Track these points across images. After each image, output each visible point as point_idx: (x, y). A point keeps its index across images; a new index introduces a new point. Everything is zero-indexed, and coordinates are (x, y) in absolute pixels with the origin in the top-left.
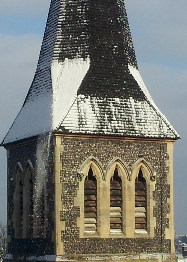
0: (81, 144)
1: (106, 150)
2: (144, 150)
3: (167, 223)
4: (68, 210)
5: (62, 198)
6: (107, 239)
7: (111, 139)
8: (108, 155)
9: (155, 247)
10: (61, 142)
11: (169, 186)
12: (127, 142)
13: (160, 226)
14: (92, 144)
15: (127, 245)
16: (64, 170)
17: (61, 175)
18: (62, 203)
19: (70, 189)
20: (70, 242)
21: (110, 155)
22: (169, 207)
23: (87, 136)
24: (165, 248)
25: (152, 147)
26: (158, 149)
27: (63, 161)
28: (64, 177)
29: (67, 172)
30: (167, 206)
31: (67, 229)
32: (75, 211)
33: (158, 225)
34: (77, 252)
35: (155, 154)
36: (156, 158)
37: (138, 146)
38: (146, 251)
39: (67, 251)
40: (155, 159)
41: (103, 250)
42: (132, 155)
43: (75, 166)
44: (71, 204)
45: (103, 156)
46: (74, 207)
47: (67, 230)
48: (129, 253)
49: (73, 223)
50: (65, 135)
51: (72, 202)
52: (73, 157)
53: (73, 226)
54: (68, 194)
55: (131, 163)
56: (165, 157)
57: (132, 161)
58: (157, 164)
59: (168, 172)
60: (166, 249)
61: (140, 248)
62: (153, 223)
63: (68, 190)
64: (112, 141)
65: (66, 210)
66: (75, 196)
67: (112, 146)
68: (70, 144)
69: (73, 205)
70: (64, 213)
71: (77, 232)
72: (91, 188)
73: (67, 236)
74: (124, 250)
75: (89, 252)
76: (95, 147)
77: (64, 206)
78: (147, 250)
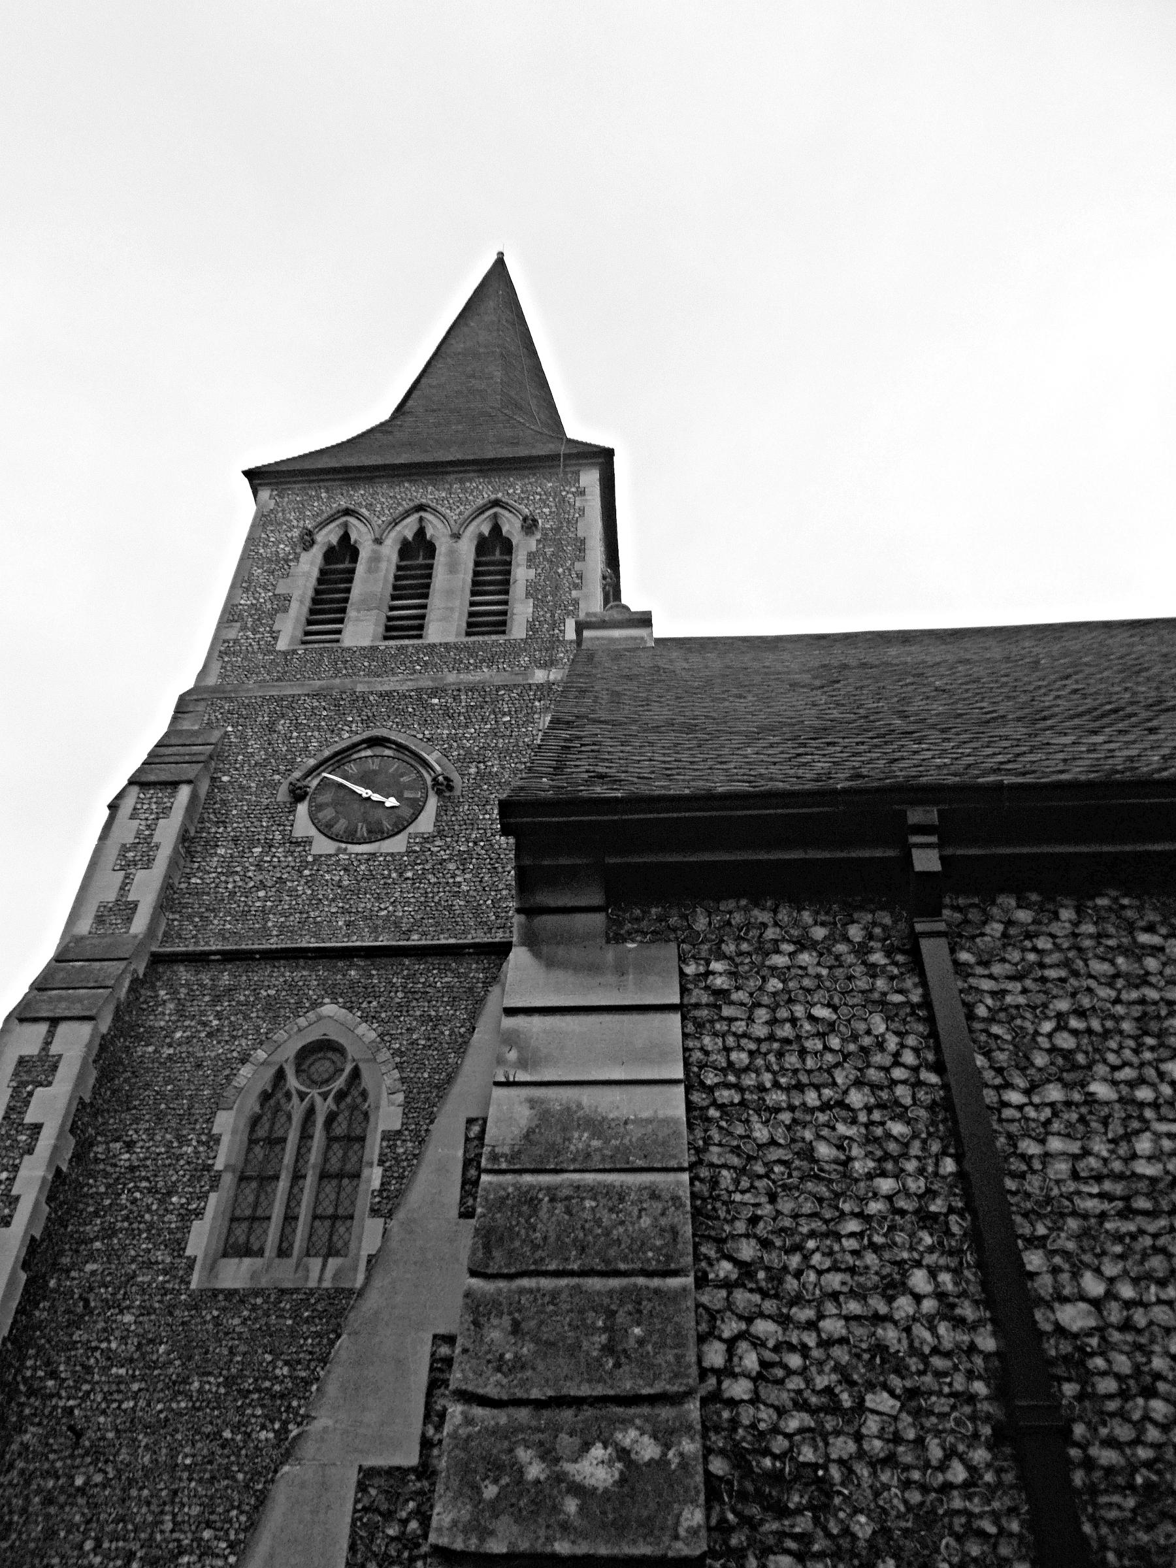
0: (323, 495)
6: (364, 648)
13: (548, 615)
14: (356, 491)
24: (562, 659)
37: (489, 483)
56: (573, 493)
58: (549, 507)
62: (522, 611)
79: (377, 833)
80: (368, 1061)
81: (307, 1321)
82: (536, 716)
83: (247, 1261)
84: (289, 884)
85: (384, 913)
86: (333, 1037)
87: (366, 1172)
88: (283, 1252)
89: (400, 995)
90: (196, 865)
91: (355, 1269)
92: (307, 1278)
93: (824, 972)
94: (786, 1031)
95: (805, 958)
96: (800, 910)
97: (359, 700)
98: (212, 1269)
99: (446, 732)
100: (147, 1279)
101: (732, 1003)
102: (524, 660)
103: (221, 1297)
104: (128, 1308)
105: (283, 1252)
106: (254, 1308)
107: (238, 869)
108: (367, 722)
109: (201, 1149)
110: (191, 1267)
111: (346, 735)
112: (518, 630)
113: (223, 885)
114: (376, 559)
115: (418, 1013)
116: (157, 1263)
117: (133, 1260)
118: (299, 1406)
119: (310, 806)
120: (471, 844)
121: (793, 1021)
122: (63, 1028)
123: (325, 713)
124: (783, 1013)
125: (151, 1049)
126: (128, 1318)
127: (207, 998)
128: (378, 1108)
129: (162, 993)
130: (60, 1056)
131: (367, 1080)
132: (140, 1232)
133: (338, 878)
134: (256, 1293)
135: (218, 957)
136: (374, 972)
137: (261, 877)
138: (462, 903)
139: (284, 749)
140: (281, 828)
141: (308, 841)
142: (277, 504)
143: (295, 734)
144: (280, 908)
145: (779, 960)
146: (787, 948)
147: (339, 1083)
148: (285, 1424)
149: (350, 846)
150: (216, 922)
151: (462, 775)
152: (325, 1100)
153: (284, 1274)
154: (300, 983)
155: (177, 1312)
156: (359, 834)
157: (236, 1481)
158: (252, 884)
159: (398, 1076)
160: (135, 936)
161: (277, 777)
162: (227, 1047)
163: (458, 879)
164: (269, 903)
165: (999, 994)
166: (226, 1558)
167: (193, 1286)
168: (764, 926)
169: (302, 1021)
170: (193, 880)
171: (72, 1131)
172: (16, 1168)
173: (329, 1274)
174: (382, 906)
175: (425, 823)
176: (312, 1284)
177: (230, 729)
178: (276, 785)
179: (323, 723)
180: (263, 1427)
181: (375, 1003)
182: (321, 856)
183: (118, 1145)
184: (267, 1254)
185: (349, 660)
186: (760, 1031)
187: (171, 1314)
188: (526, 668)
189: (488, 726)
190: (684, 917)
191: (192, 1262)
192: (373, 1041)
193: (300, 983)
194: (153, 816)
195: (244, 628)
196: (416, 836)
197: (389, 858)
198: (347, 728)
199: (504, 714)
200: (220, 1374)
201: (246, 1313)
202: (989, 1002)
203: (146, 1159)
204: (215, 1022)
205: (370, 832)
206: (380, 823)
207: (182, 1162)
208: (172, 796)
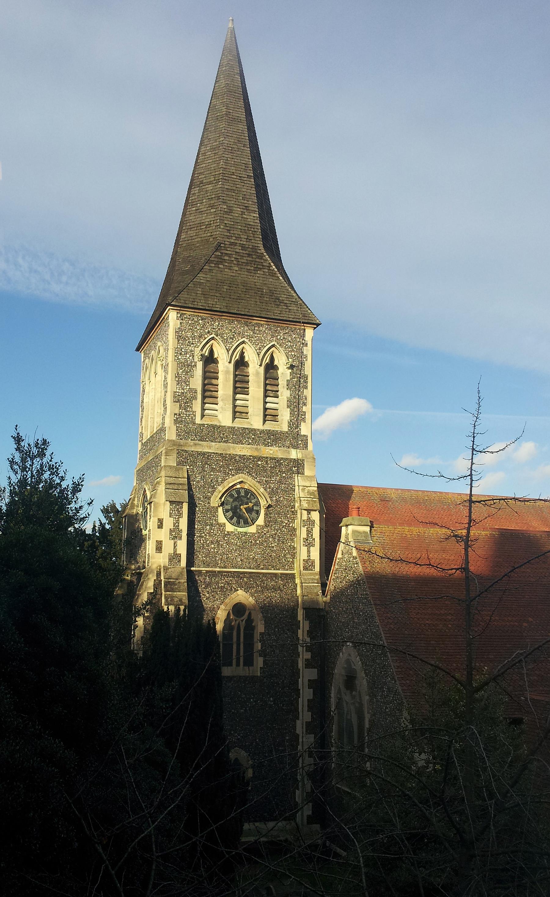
0: (200, 321)
1: (231, 331)
2: (277, 334)
3: (303, 417)
5: (176, 377)
6: (229, 427)
7: (237, 319)
9: (288, 442)
10: (177, 317)
11: (307, 376)
12: (256, 324)
15: (253, 437)
16: (179, 347)
17: (175, 353)
18: (176, 383)
19: (187, 369)
20: (184, 426)
21: (235, 335)
23: (208, 312)
24: (300, 444)
25: (287, 331)
26: (294, 334)
28: (179, 355)
29: (183, 350)
30: (304, 398)
31: (181, 412)
32: (191, 393)
33: (293, 418)
34: (192, 438)
35: (290, 339)
37: (270, 329)
38: (277, 445)
39: (180, 435)
40: (290, 345)
41: (224, 440)
42: (263, 338)
43: (192, 344)
44: (186, 385)
45: (228, 336)
46: (190, 388)
47: (180, 413)
48: (256, 445)
49: (188, 406)
50: (181, 309)
51: (187, 383)
52: (191, 334)
53: (188, 409)
54: (184, 373)
55: (261, 346)
57: (262, 344)
58: (293, 351)
59: (307, 360)
60: (301, 445)
63: (183, 369)
64: (237, 320)
65: (180, 391)
66: (192, 376)
67: (239, 326)
68: (188, 320)
69: (189, 386)
70: (177, 394)
71: (192, 415)
72: (212, 370)
73: (181, 419)
74: (250, 441)
75: (207, 439)
77: (178, 386)
78: (278, 444)
79: (246, 524)
81: (247, 684)
84: (221, 543)
85: (251, 557)
87: (256, 645)
88: (238, 665)
97: (232, 457)
99: (264, 479)
107: (203, 535)
111: (231, 476)
113: (199, 541)
114: (227, 372)
115: (265, 595)
118: (248, 705)
119: (223, 510)
120: (276, 531)
127: (203, 586)
134: (234, 677)
136: (251, 579)
138: (275, 555)
139: (210, 480)
140: (214, 518)
141: (224, 524)
143: (212, 473)
144: (219, 552)
147: (245, 617)
148: (246, 708)
149: (238, 528)
150: (200, 556)
152: (242, 621)
156: (241, 524)
157: (237, 721)
158: (208, 542)
159: (262, 615)
162: (212, 604)
163: (273, 545)
166: (237, 737)
174: (251, 554)
175: (261, 521)
177: (188, 467)
179: (221, 469)
180: (241, 709)
181: (253, 590)
182: (229, 532)
189: (278, 478)
192: (254, 603)
197: (251, 535)
199: (284, 472)
200: (229, 697)
204: (208, 595)
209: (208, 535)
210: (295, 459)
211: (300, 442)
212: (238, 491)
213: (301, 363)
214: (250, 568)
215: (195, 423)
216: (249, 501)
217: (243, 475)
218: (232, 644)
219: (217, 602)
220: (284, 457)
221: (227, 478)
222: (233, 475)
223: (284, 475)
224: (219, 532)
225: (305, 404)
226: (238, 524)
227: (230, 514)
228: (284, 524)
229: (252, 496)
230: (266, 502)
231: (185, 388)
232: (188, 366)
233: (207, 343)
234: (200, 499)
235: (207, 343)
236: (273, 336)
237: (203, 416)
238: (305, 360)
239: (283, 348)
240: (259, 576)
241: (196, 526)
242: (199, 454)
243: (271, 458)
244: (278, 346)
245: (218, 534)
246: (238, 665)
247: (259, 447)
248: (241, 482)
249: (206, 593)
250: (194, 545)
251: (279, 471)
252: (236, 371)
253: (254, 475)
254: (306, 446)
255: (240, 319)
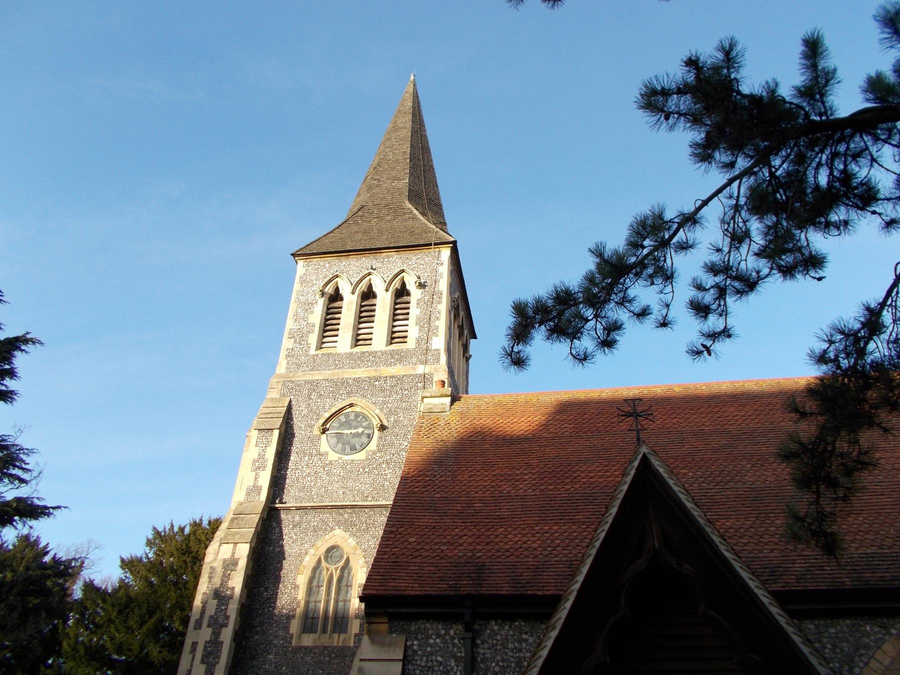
0: (327, 265)
1: (358, 267)
4: (299, 327)
8: (360, 271)
15: (373, 359)
18: (293, 321)
22: (439, 313)
27: (303, 281)
36: (425, 267)
37: (401, 258)
42: (392, 267)
53: (303, 343)
61: (392, 360)
65: (297, 328)
71: (307, 348)
76: (345, 265)
79: (354, 449)
80: (353, 554)
82: (419, 391)
83: (311, 635)
85: (357, 488)
86: (339, 543)
87: (352, 601)
89: (364, 525)
90: (283, 465)
91: (350, 639)
92: (333, 642)
93: (442, 645)
94: (430, 664)
95: (438, 640)
96: (438, 624)
97: (344, 382)
98: (299, 638)
99: (382, 399)
100: (276, 642)
101: (417, 655)
102: (414, 360)
103: (303, 649)
104: (271, 653)
105: (324, 631)
106: (315, 653)
108: (349, 394)
109: (293, 591)
110: (291, 638)
111: (340, 401)
112: (411, 343)
113: (294, 474)
114: (350, 303)
115: (371, 533)
116: (280, 636)
117: (271, 634)
120: (392, 456)
121: (432, 661)
122: (239, 545)
123: (331, 389)
124: (430, 659)
125: (271, 548)
126: (271, 657)
127: (291, 526)
128: (357, 574)
129: (274, 524)
130: (239, 559)
131: (352, 563)
132: (273, 625)
133: (338, 472)
134: (315, 647)
135: (294, 508)
137: (308, 471)
140: (315, 447)
141: (327, 454)
142: (306, 270)
143: (319, 400)
145: (431, 641)
146: (434, 637)
147: (342, 564)
150: (292, 492)
151: (388, 421)
153: (325, 640)
154: (326, 520)
155: (288, 655)
156: (346, 451)
158: (305, 474)
160: (262, 502)
161: (313, 422)
163: (387, 472)
164: (312, 483)
165: (484, 654)
167: (293, 645)
168: (429, 629)
169: (327, 537)
170: (282, 472)
171: (246, 587)
172: (227, 604)
173: (341, 640)
174: (357, 485)
175: (373, 446)
176: (335, 644)
177: (292, 397)
178: (312, 426)
181: (354, 529)
183: (262, 589)
184: (319, 632)
185: (339, 361)
186: (423, 664)
187: (286, 655)
188: (415, 364)
190: (408, 625)
191: (292, 635)
193: (326, 520)
194: (265, 445)
195: (295, 342)
196: (370, 451)
197: (359, 462)
198: (340, 397)
201: (312, 655)
202: (481, 656)
203: (273, 594)
204: (295, 537)
205: (351, 450)
206: (354, 445)
207: (286, 596)
208: (271, 435)
209: (305, 467)
210: (421, 374)
211: (430, 357)
212: (347, 415)
213: (435, 281)
214: (354, 501)
215: (307, 355)
216: (358, 424)
217: (356, 398)
218: (320, 602)
219: (306, 546)
220: (408, 374)
221: (336, 403)
222: (344, 399)
223: (406, 392)
224: (319, 462)
225: (437, 319)
226: (343, 452)
227: (334, 440)
228: (403, 447)
229: (363, 419)
230: (379, 422)
231: (303, 323)
232: (308, 304)
233: (330, 281)
234: (300, 428)
235: (330, 281)
236: (403, 263)
237: (319, 347)
238: (439, 277)
239: (415, 272)
240: (365, 511)
241: (292, 458)
242: (307, 382)
243: (390, 377)
244: (407, 270)
245: (317, 465)
246: (324, 631)
247: (379, 368)
248: (351, 405)
249: (293, 535)
250: (285, 479)
251: (401, 389)
252: (362, 302)
253: (369, 396)
254: (438, 360)
255: (368, 255)
